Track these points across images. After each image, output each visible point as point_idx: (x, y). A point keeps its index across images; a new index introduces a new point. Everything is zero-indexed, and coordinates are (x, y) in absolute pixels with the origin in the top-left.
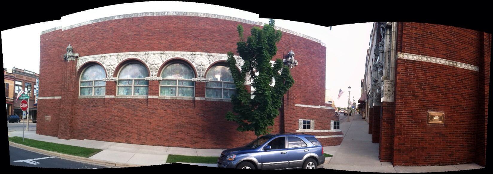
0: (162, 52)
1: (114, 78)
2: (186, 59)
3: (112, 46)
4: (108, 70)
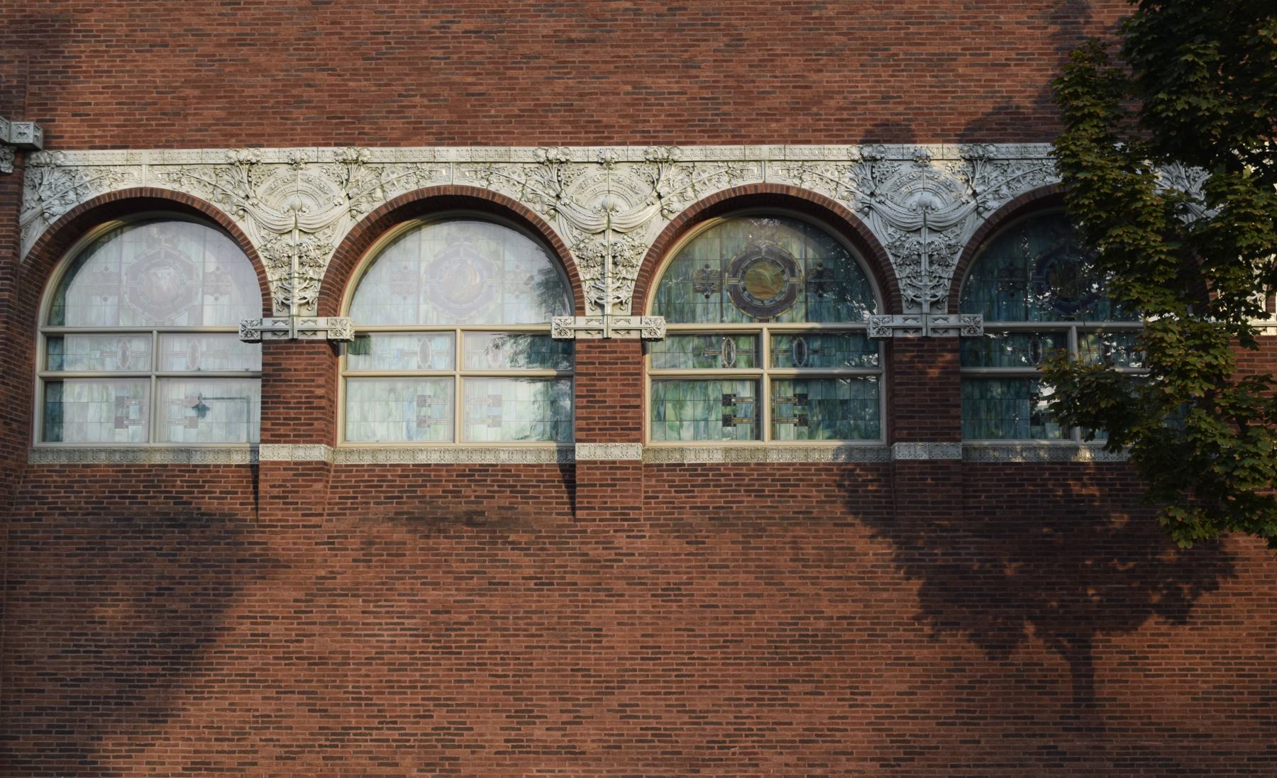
0: (661, 152)
1: (322, 322)
2: (822, 190)
3: (307, 93)
4: (277, 263)
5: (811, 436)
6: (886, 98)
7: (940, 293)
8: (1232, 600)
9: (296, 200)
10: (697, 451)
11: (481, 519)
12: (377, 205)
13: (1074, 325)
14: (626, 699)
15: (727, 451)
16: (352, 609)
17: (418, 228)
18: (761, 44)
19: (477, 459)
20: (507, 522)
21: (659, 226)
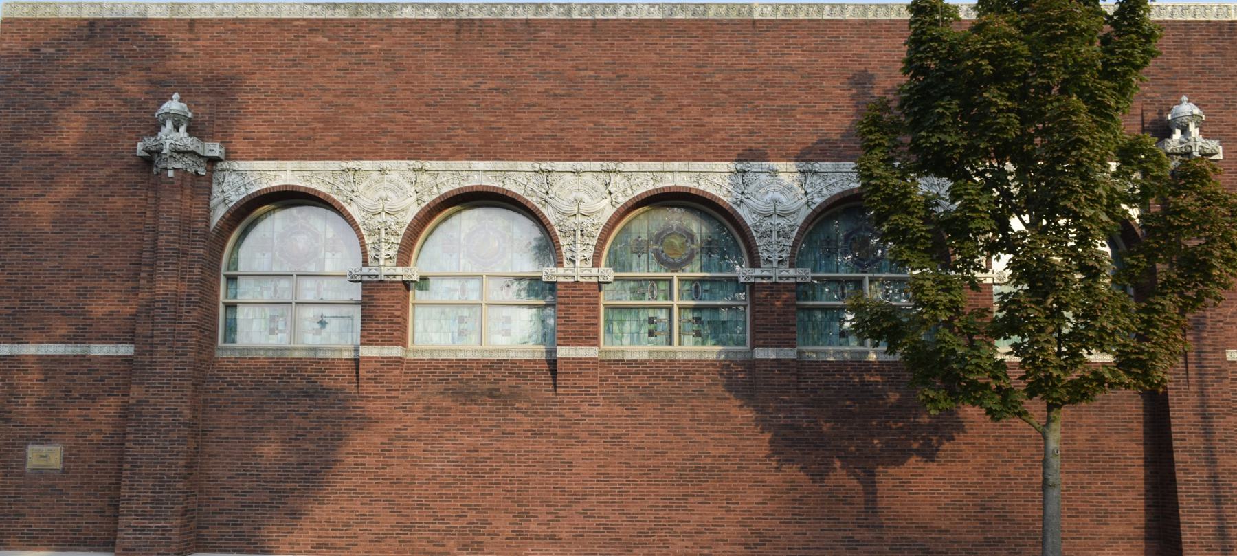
1: (399, 270)
3: (391, 127)
4: (371, 232)
5: (703, 343)
6: (751, 133)
7: (784, 255)
8: (963, 447)
9: (383, 194)
10: (632, 352)
11: (497, 393)
12: (434, 197)
13: (867, 275)
14: (587, 506)
15: (651, 352)
16: (417, 449)
17: (460, 211)
18: (674, 98)
19: (495, 356)
20: (514, 395)
21: (609, 212)
